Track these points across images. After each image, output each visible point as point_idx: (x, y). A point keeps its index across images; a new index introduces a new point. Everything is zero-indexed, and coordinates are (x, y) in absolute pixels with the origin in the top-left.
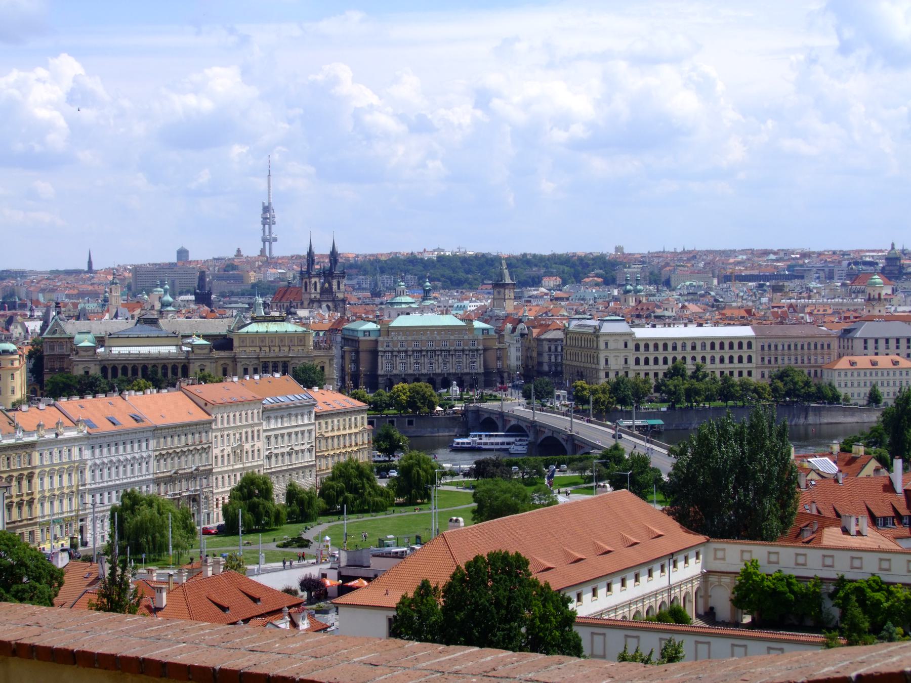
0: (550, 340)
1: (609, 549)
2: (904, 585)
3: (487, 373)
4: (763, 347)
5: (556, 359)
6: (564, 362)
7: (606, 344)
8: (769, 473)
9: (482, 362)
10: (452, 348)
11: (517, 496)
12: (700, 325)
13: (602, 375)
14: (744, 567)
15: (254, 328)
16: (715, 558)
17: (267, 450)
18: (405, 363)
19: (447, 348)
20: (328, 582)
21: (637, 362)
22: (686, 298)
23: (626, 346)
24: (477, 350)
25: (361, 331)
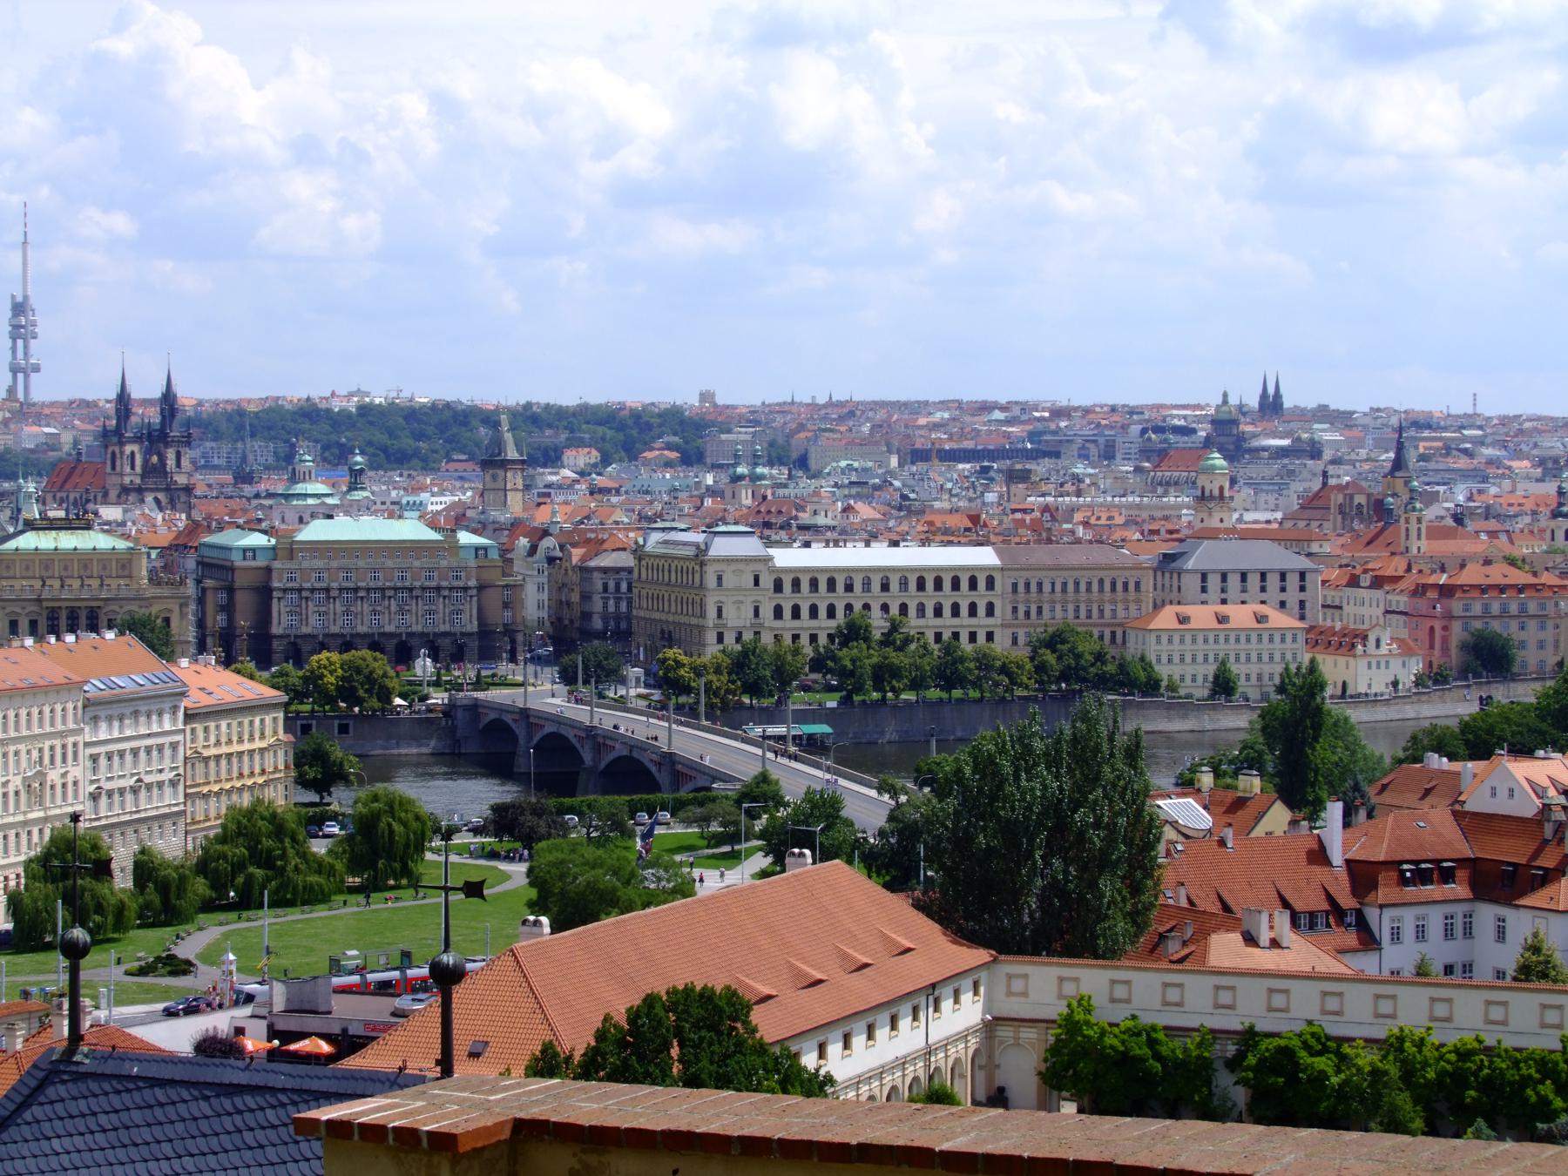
0: (605, 570)
1: (819, 976)
2: (1367, 1040)
3: (485, 633)
4: (1015, 586)
5: (617, 606)
6: (635, 612)
7: (720, 578)
8: (1112, 828)
9: (475, 612)
10: (417, 584)
11: (615, 873)
12: (895, 544)
13: (711, 637)
14: (1065, 1011)
15: (28, 541)
16: (1009, 993)
17: (92, 782)
18: (325, 613)
19: (407, 584)
20: (250, 1045)
21: (778, 612)
22: (846, 492)
23: (757, 582)
24: (465, 589)
25: (238, 549)
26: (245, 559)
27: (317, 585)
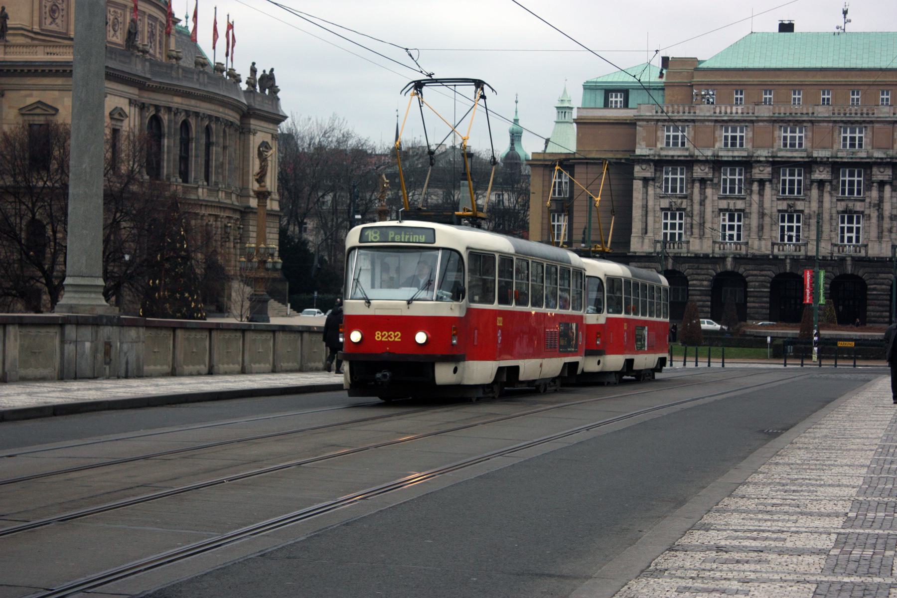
18: (742, 213)
26: (606, 105)
27: (726, 155)
